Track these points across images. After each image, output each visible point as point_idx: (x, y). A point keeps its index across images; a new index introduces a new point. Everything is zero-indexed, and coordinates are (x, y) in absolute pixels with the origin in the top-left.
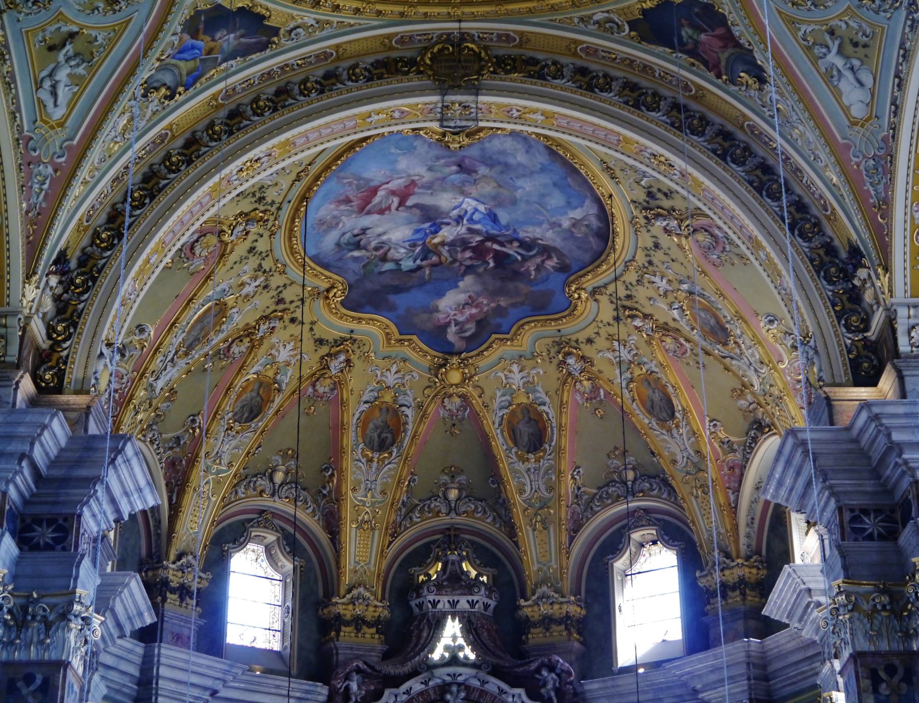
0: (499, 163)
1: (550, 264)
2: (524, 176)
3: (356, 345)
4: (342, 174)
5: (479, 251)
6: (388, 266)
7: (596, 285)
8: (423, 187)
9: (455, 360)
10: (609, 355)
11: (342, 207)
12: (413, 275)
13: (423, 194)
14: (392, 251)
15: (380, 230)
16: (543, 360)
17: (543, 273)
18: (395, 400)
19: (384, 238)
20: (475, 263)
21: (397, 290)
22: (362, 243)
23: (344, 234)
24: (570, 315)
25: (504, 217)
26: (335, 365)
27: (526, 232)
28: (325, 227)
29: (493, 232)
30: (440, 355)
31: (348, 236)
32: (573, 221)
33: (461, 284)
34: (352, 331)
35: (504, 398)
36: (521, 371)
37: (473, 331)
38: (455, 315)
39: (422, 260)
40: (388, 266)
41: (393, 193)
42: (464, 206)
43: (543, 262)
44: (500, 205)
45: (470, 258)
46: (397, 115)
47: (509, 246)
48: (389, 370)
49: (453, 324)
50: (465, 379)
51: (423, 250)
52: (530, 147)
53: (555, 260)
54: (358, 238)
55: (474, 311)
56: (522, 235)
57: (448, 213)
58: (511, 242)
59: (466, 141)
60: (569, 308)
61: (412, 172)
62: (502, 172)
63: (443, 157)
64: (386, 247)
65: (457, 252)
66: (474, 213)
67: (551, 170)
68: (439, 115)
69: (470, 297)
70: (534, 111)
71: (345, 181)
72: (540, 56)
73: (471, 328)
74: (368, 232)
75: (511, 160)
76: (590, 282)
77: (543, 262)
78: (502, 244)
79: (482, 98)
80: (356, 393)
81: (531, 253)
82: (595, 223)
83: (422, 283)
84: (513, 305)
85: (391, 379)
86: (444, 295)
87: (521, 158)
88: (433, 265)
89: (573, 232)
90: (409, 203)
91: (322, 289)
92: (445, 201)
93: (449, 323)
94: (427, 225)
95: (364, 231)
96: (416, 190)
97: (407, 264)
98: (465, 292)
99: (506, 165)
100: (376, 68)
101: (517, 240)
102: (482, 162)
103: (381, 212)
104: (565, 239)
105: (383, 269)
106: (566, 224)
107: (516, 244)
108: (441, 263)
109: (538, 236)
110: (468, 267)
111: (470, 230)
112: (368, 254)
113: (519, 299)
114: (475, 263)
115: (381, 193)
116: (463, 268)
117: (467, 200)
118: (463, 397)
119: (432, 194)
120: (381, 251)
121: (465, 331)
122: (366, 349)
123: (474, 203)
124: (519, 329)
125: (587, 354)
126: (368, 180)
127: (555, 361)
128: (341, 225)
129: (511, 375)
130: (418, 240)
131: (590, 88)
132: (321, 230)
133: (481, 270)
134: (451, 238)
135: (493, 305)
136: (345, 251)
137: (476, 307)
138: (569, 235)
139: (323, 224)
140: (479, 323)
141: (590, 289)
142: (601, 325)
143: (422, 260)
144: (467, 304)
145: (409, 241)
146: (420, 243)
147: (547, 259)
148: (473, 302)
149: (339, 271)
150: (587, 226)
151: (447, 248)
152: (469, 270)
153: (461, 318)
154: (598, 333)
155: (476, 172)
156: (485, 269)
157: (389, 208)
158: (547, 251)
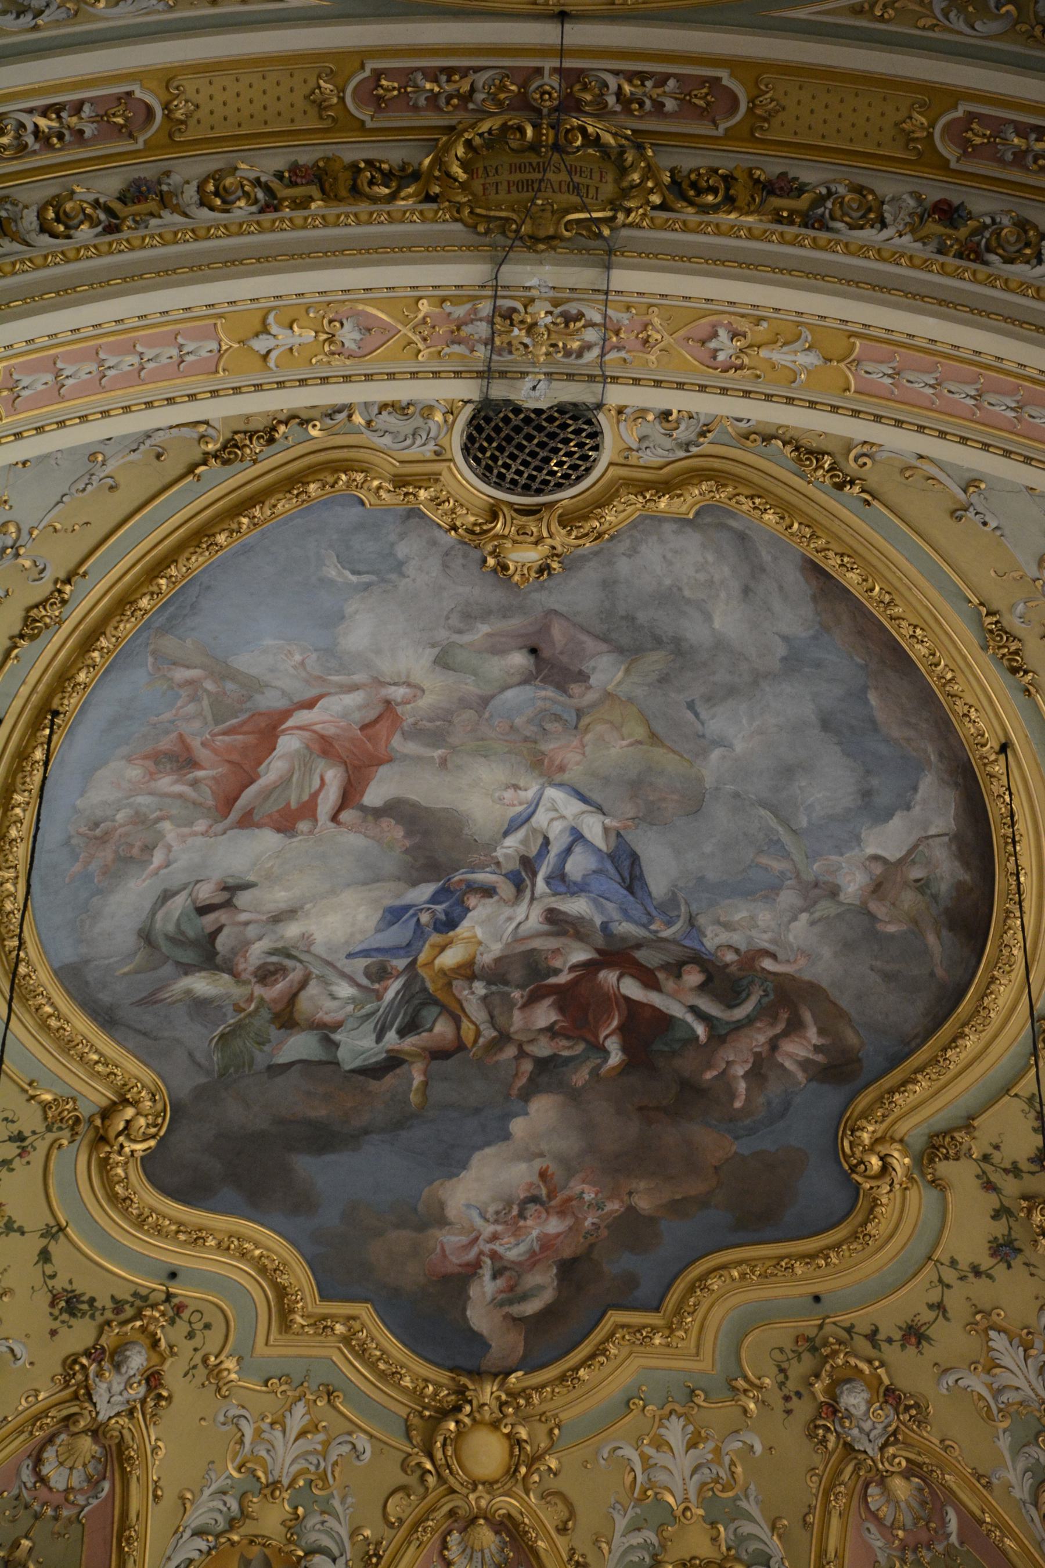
0: (658, 642)
1: (796, 1051)
2: (731, 691)
3: (182, 1327)
4: (169, 644)
5: (580, 1005)
6: (299, 1046)
7: (939, 1123)
8: (416, 733)
9: (488, 1393)
10: (976, 1383)
11: (166, 783)
12: (373, 1085)
13: (418, 759)
14: (313, 989)
15: (279, 897)
16: (762, 1403)
17: (774, 1089)
18: (294, 1525)
19: (292, 930)
20: (565, 1049)
21: (323, 1138)
22: (222, 943)
23: (166, 896)
24: (854, 1236)
25: (661, 870)
26: (112, 1394)
27: (727, 926)
28: (107, 854)
29: (625, 928)
30: (444, 1377)
31: (179, 904)
32: (878, 869)
33: (518, 1126)
34: (173, 1275)
35: (636, 1539)
36: (692, 1445)
37: (547, 1296)
38: (495, 1237)
39: (402, 1033)
40: (299, 1046)
41: (325, 747)
42: (541, 819)
43: (774, 1045)
44: (650, 816)
45: (551, 1031)
46: (348, 335)
47: (670, 985)
48: (279, 1422)
49: (486, 1272)
50: (521, 1460)
51: (407, 994)
52: (758, 570)
53: (812, 1034)
54: (209, 921)
55: (554, 1226)
56: (713, 938)
57: (491, 846)
58: (676, 969)
59: (561, 538)
60: (851, 1201)
61: (386, 667)
62: (664, 680)
63: (486, 614)
64: (295, 976)
65: (509, 1004)
66: (568, 851)
67: (818, 664)
68: (481, 352)
69: (543, 1175)
70: (791, 331)
71: (181, 674)
72: (809, 175)
73: (543, 1287)
74: (243, 899)
75: (695, 632)
76: (921, 1105)
77: (774, 1045)
78: (650, 982)
79: (627, 279)
80: (169, 1496)
81: (740, 1013)
82: (946, 870)
83: (402, 1120)
84: (677, 1208)
85: (285, 1457)
86: (464, 1165)
87: (727, 620)
88: (438, 1054)
89: (872, 917)
90: (374, 795)
91: (84, 1112)
92: (482, 794)
93: (476, 1266)
94: (427, 890)
95: (232, 889)
96: (397, 742)
97: (359, 1046)
98: (530, 1156)
99: (679, 649)
100: (293, 184)
101: (698, 959)
102: (604, 639)
103: (285, 824)
104: (848, 947)
105: (282, 1059)
106: (853, 884)
107: (693, 977)
108: (460, 1047)
109: (763, 941)
110: (543, 1064)
111: (553, 917)
112: (238, 992)
113: (696, 1187)
114: (565, 1049)
115: (289, 743)
116: (527, 1066)
117: (551, 792)
118: (509, 1528)
119: (444, 762)
120: (280, 987)
121: (524, 1298)
122: (212, 1341)
123: (572, 807)
124: (691, 1290)
125: (904, 1384)
126: (254, 686)
127: (804, 1409)
128: (158, 857)
129: (661, 1458)
130: (394, 951)
131: (972, 252)
132: (93, 867)
133: (580, 1077)
134: (496, 949)
135: (614, 1206)
136: (168, 969)
137: (562, 1213)
138: (861, 930)
139: (103, 840)
140: (572, 1271)
141: (918, 1142)
142: (949, 1275)
143: (402, 1033)
144: (534, 1199)
145: (365, 953)
146: (401, 963)
147: (785, 1034)
148: (551, 1195)
149: (149, 1045)
150: (922, 886)
151: (480, 988)
152: (547, 1073)
153: (513, 1252)
154: (939, 1307)
155: (582, 677)
156: (595, 1073)
157: (308, 810)
158: (789, 1000)
